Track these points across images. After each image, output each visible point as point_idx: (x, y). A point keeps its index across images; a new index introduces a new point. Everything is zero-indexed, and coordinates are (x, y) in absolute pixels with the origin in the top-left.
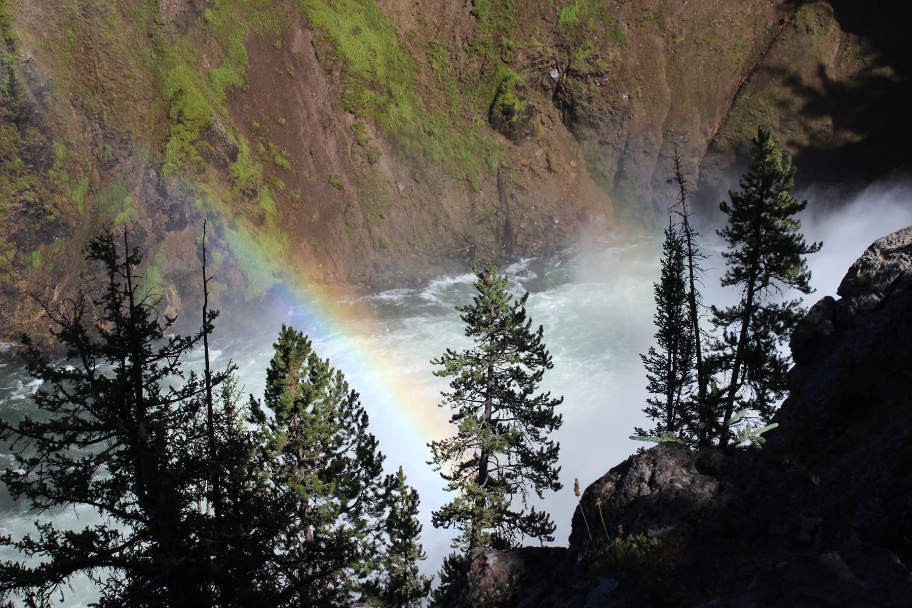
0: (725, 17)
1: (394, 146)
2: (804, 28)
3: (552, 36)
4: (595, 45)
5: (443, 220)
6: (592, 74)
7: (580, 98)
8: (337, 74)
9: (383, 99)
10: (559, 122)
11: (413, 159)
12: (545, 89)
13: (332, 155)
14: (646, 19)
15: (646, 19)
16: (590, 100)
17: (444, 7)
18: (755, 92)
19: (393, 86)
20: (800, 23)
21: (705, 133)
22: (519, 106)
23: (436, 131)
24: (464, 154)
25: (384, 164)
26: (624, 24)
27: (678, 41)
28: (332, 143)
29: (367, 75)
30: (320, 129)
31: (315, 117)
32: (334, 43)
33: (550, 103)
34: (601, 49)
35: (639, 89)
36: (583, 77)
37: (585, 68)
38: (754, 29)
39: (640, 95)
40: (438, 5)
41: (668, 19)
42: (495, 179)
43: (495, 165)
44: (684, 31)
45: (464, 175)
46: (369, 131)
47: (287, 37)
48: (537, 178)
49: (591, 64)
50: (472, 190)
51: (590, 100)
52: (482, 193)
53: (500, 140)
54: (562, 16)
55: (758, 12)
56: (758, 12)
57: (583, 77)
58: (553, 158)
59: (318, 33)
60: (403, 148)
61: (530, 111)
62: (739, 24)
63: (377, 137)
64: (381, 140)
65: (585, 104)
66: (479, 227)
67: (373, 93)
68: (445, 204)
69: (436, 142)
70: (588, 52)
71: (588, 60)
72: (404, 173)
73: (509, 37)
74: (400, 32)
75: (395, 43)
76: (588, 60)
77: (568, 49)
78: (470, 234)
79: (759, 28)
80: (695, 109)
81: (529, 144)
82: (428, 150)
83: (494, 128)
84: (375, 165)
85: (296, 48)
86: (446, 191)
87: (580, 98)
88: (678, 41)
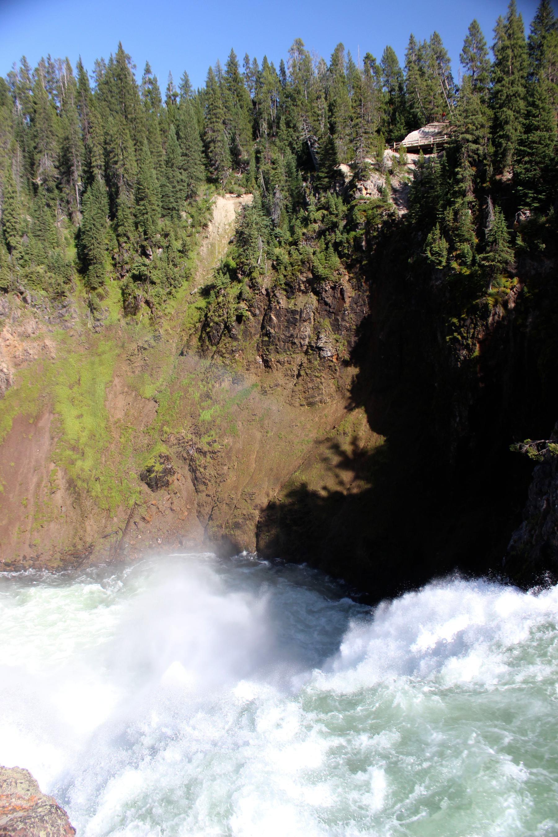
0: (300, 422)
1: (70, 485)
2: (342, 432)
3: (194, 427)
4: (216, 434)
5: (81, 533)
6: (209, 452)
7: (199, 466)
8: (56, 440)
9: (75, 457)
10: (189, 480)
11: (79, 495)
12: (185, 459)
13: (32, 487)
14: (253, 420)
15: (253, 420)
16: (205, 468)
17: (143, 407)
18: (302, 471)
19: (87, 449)
20: (341, 429)
21: (268, 495)
22: (158, 468)
23: (102, 478)
24: (113, 494)
25: (59, 496)
26: (240, 423)
27: (268, 435)
28: (35, 480)
29: (72, 442)
30: (32, 471)
31: (33, 463)
32: (62, 422)
33: (187, 468)
34: (219, 437)
35: (236, 464)
36: (205, 454)
37: (206, 448)
38: (318, 431)
39: (236, 467)
40: (141, 406)
41: (266, 422)
42: (129, 511)
43: (132, 502)
44: (274, 429)
45: (107, 507)
46: (60, 474)
47: (38, 418)
48: (160, 514)
49: (210, 445)
50: (109, 517)
51: (205, 468)
52: (115, 519)
53: (145, 488)
54: (202, 415)
55: (322, 421)
56: (322, 421)
57: (205, 454)
58: (176, 501)
59: (56, 416)
60: (76, 486)
61: (169, 472)
62: (309, 427)
63: (63, 478)
64: (64, 480)
65: (202, 470)
66: (102, 540)
67: (71, 453)
68: (87, 523)
69: (98, 486)
70: (210, 438)
71: (209, 444)
72: (69, 502)
73: (168, 426)
74: (111, 419)
75: (103, 425)
76: (209, 444)
77: (200, 435)
78: (94, 544)
79: (320, 430)
80: (266, 479)
81: (162, 491)
82: (90, 490)
83: (142, 480)
84: (53, 495)
85: (41, 424)
86: (91, 515)
87: (199, 466)
88: (268, 435)
